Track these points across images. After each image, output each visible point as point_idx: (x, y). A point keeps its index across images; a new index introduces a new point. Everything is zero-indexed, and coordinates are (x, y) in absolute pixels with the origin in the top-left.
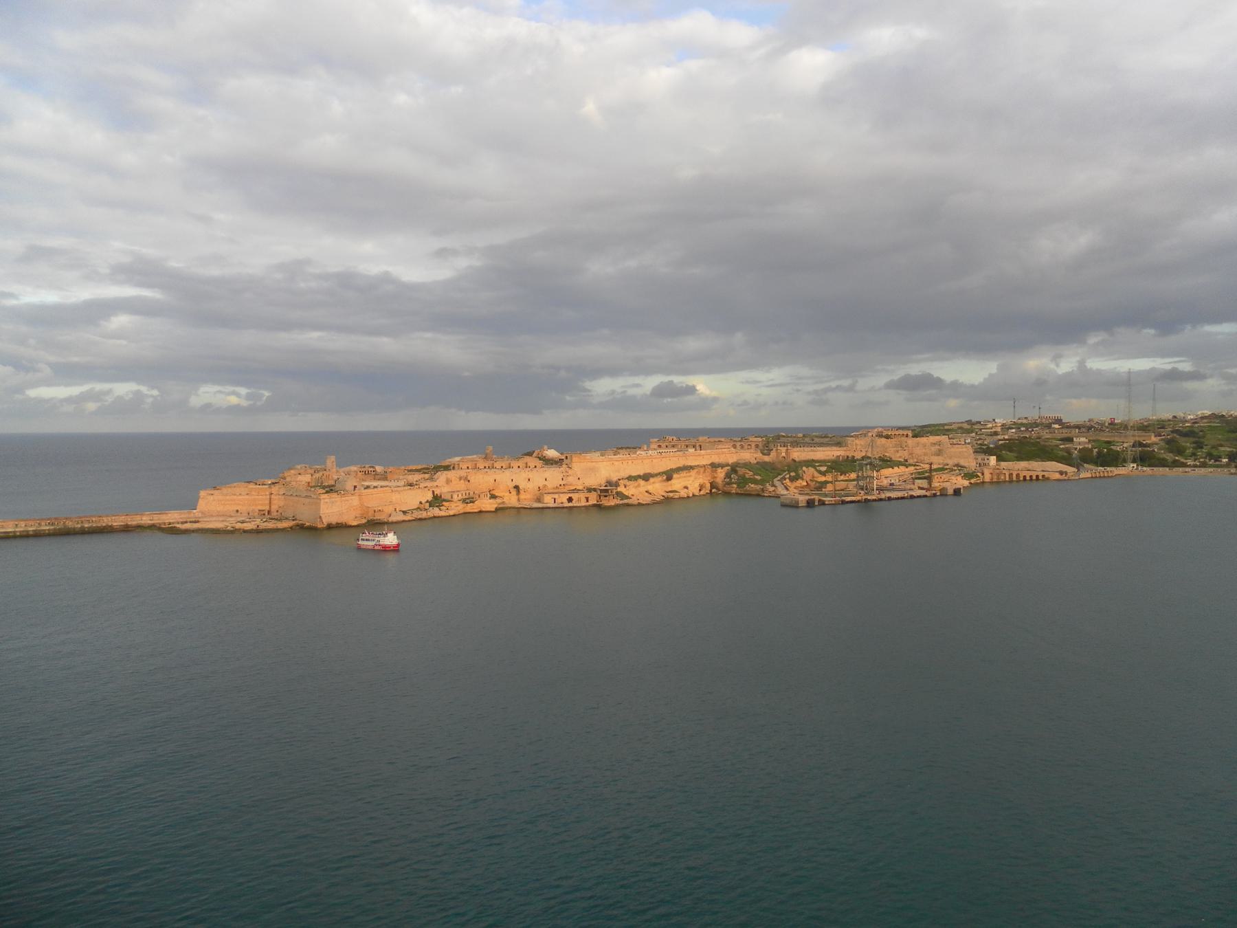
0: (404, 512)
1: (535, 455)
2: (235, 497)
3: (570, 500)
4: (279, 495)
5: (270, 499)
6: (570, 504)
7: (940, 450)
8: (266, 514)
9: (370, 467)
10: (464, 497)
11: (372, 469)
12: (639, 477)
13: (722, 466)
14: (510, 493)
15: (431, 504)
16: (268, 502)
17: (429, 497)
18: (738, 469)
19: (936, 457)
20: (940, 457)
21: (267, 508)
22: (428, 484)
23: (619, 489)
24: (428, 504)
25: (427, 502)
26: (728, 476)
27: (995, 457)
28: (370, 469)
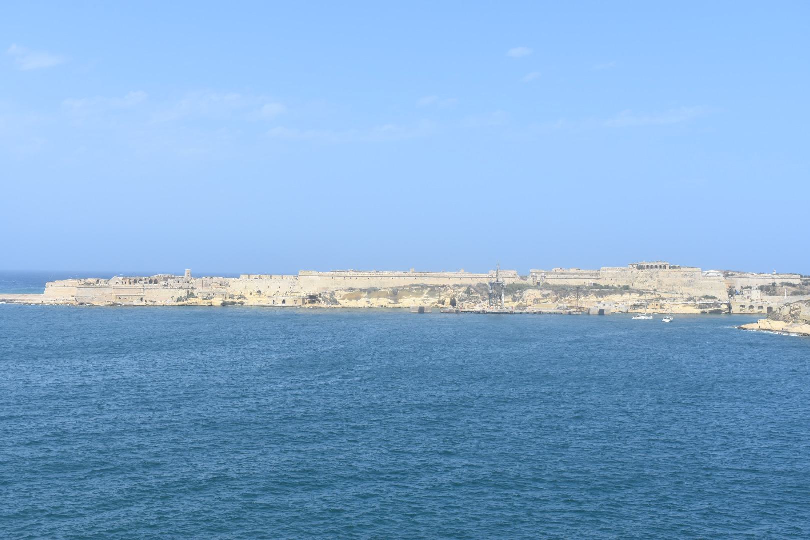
3: (284, 302)
6: (284, 305)
7: (690, 282)
12: (361, 290)
19: (686, 288)
20: (691, 288)
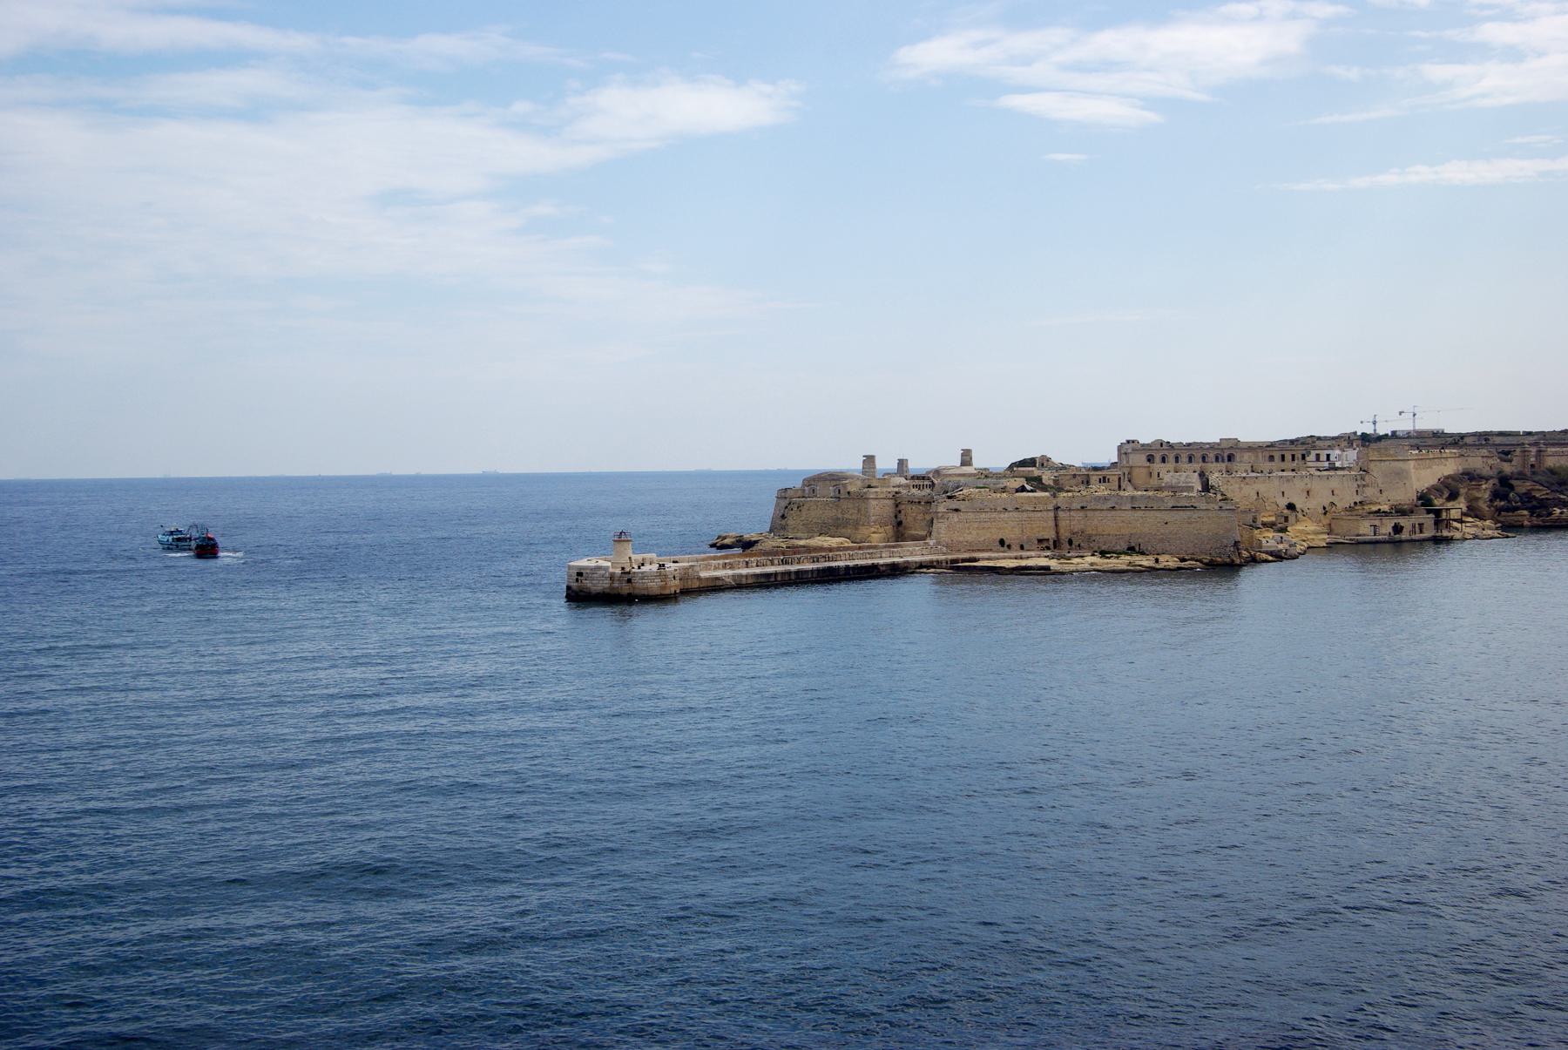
2: (994, 515)
3: (1398, 529)
5: (1056, 517)
8: (1052, 547)
16: (1052, 523)
18: (1513, 482)
21: (1051, 535)
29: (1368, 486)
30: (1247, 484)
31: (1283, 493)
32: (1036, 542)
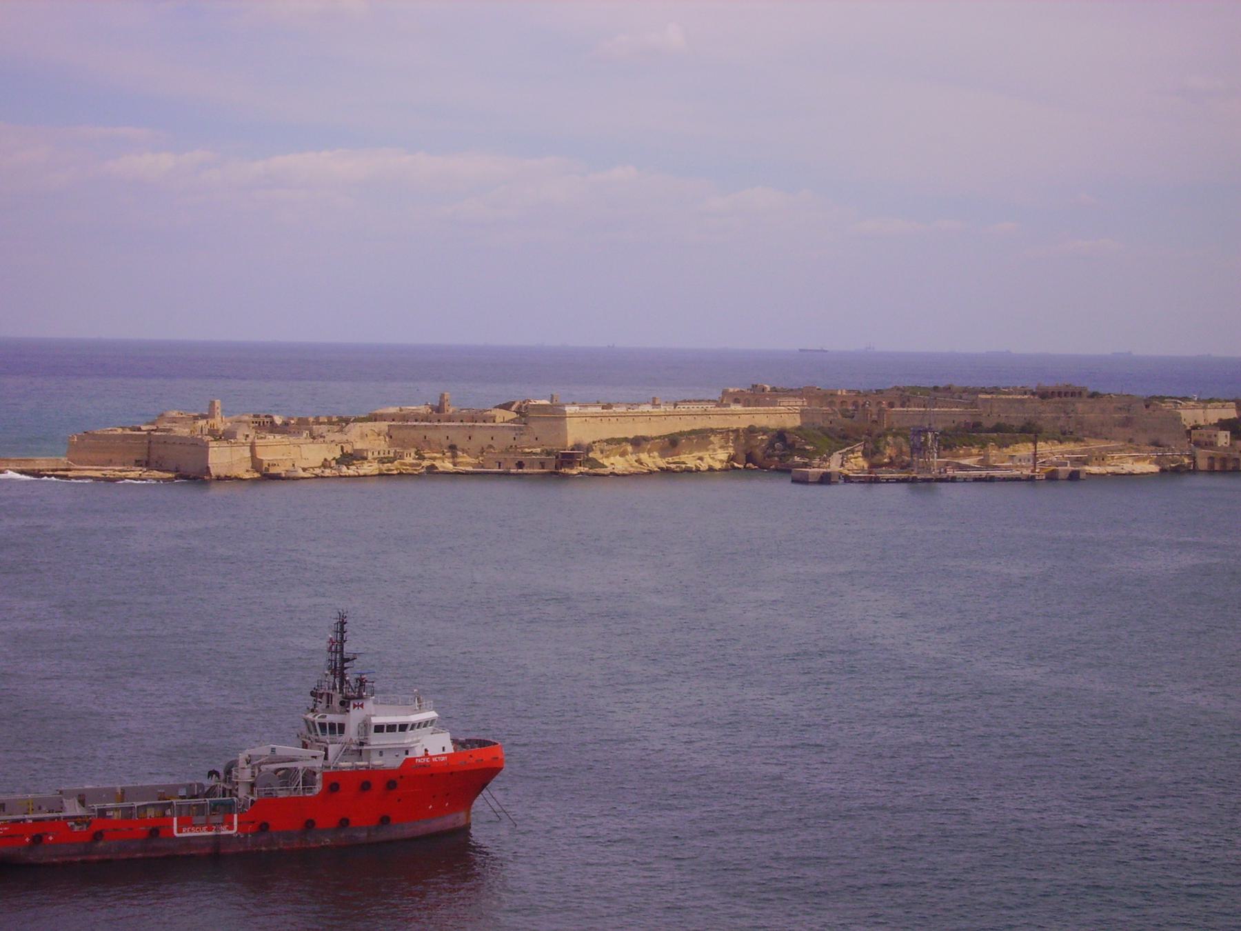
0: (304, 470)
1: (514, 408)
4: (159, 443)
5: (149, 448)
9: (266, 416)
10: (382, 455)
11: (268, 419)
12: (626, 440)
13: (764, 431)
14: (444, 454)
15: (338, 462)
17: (338, 455)
21: (145, 458)
22: (338, 437)
23: (591, 455)
24: (334, 462)
25: (334, 459)
26: (771, 445)
27: (1228, 433)
28: (266, 420)
29: (525, 435)
30: (415, 430)
31: (448, 437)
32: (134, 461)
